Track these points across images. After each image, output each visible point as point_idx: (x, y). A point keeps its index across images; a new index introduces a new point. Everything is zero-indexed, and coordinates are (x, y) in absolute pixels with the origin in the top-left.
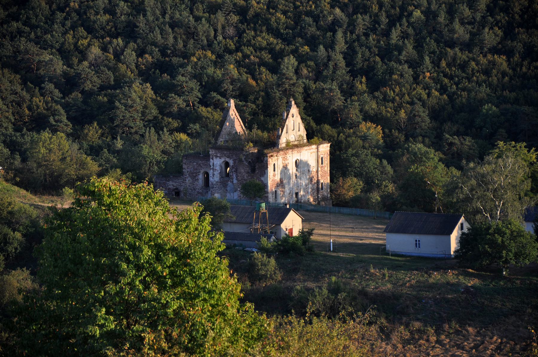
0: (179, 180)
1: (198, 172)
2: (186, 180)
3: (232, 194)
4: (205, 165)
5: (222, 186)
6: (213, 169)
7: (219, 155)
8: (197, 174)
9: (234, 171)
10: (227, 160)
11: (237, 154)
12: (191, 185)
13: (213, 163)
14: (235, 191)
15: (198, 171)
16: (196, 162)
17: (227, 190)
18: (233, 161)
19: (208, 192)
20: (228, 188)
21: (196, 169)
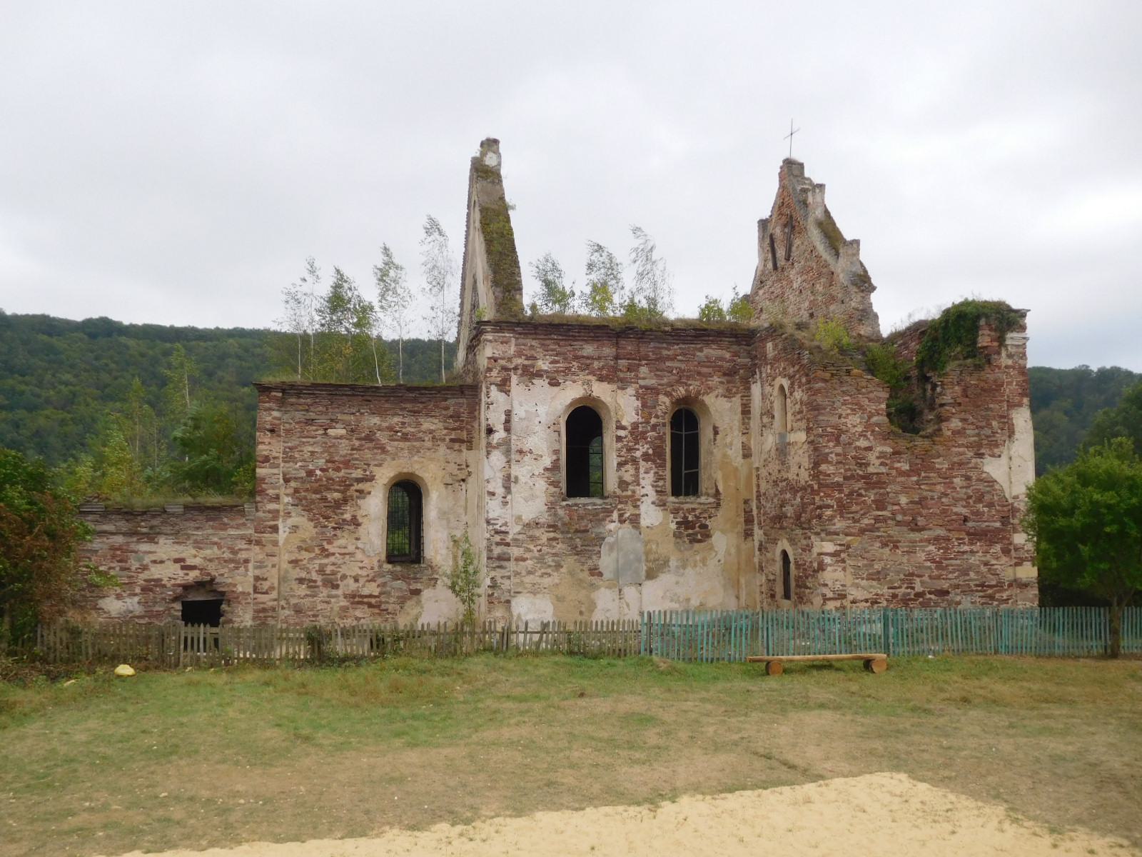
0: (224, 527)
1: (359, 480)
2: (275, 529)
3: (630, 592)
4: (405, 438)
5: (560, 547)
6: (506, 445)
7: (543, 365)
8: (350, 492)
9: (646, 457)
10: (602, 391)
11: (662, 359)
12: (306, 555)
13: (508, 414)
14: (651, 575)
15: (358, 473)
16: (347, 424)
17: (596, 572)
18: (638, 396)
19: (417, 592)
20: (606, 561)
21: (347, 464)
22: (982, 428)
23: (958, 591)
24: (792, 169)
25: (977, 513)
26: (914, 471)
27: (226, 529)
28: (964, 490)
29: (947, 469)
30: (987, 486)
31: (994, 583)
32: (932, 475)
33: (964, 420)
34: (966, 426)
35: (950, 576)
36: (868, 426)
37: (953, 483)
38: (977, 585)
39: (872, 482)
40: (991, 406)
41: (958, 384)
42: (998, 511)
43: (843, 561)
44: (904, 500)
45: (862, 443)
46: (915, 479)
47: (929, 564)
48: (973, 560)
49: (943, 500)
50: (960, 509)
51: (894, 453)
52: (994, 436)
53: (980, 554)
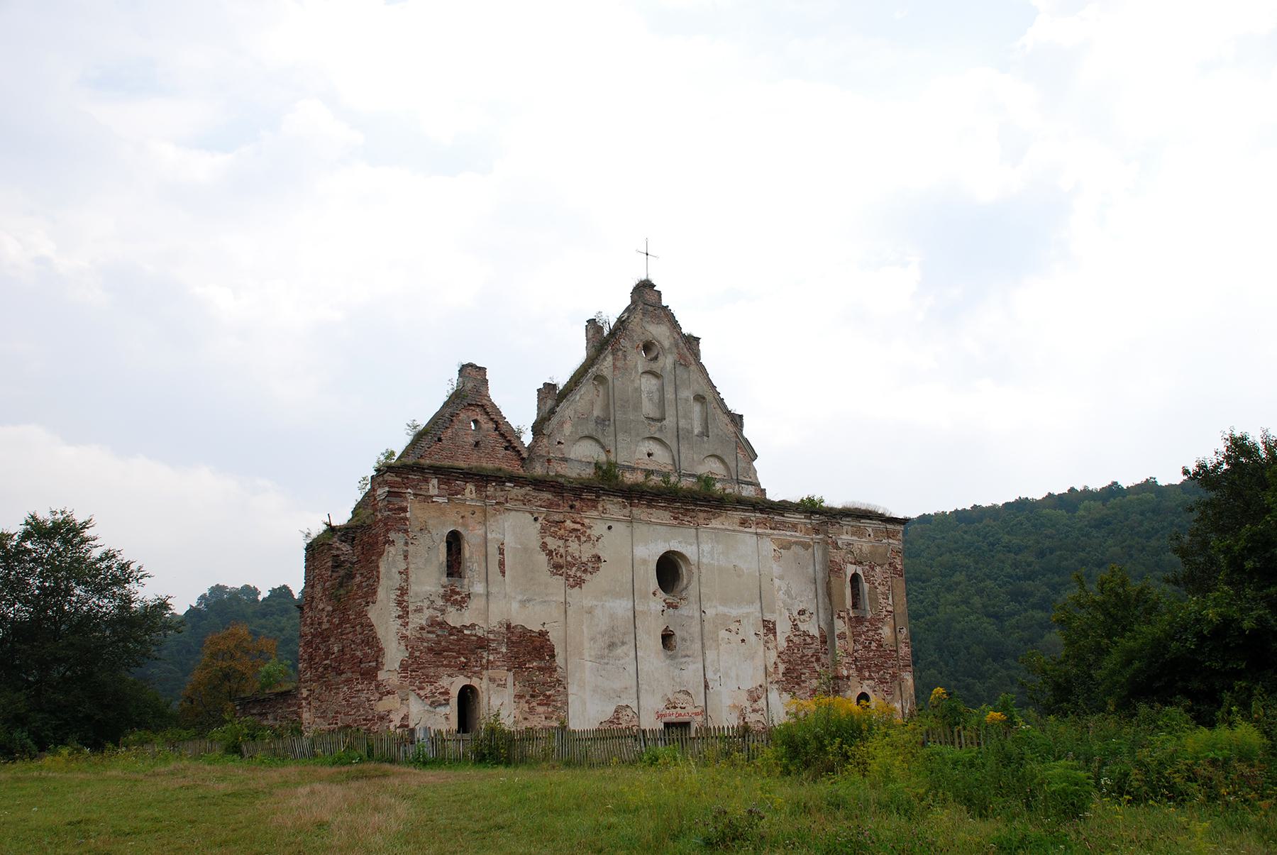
0: (289, 706)
22: (369, 578)
23: (356, 725)
24: (645, 293)
25: (365, 655)
26: (341, 624)
27: (289, 708)
28: (361, 636)
29: (354, 619)
30: (370, 631)
31: (371, 717)
32: (348, 625)
33: (362, 574)
34: (363, 580)
35: (353, 713)
36: (324, 590)
37: (356, 630)
38: (364, 720)
39: (324, 636)
40: (373, 558)
41: (360, 544)
42: (375, 652)
43: (309, 703)
44: (336, 649)
45: (320, 607)
46: (340, 630)
47: (344, 702)
48: (363, 696)
49: (353, 646)
50: (359, 653)
51: (333, 611)
52: (373, 585)
53: (365, 692)
